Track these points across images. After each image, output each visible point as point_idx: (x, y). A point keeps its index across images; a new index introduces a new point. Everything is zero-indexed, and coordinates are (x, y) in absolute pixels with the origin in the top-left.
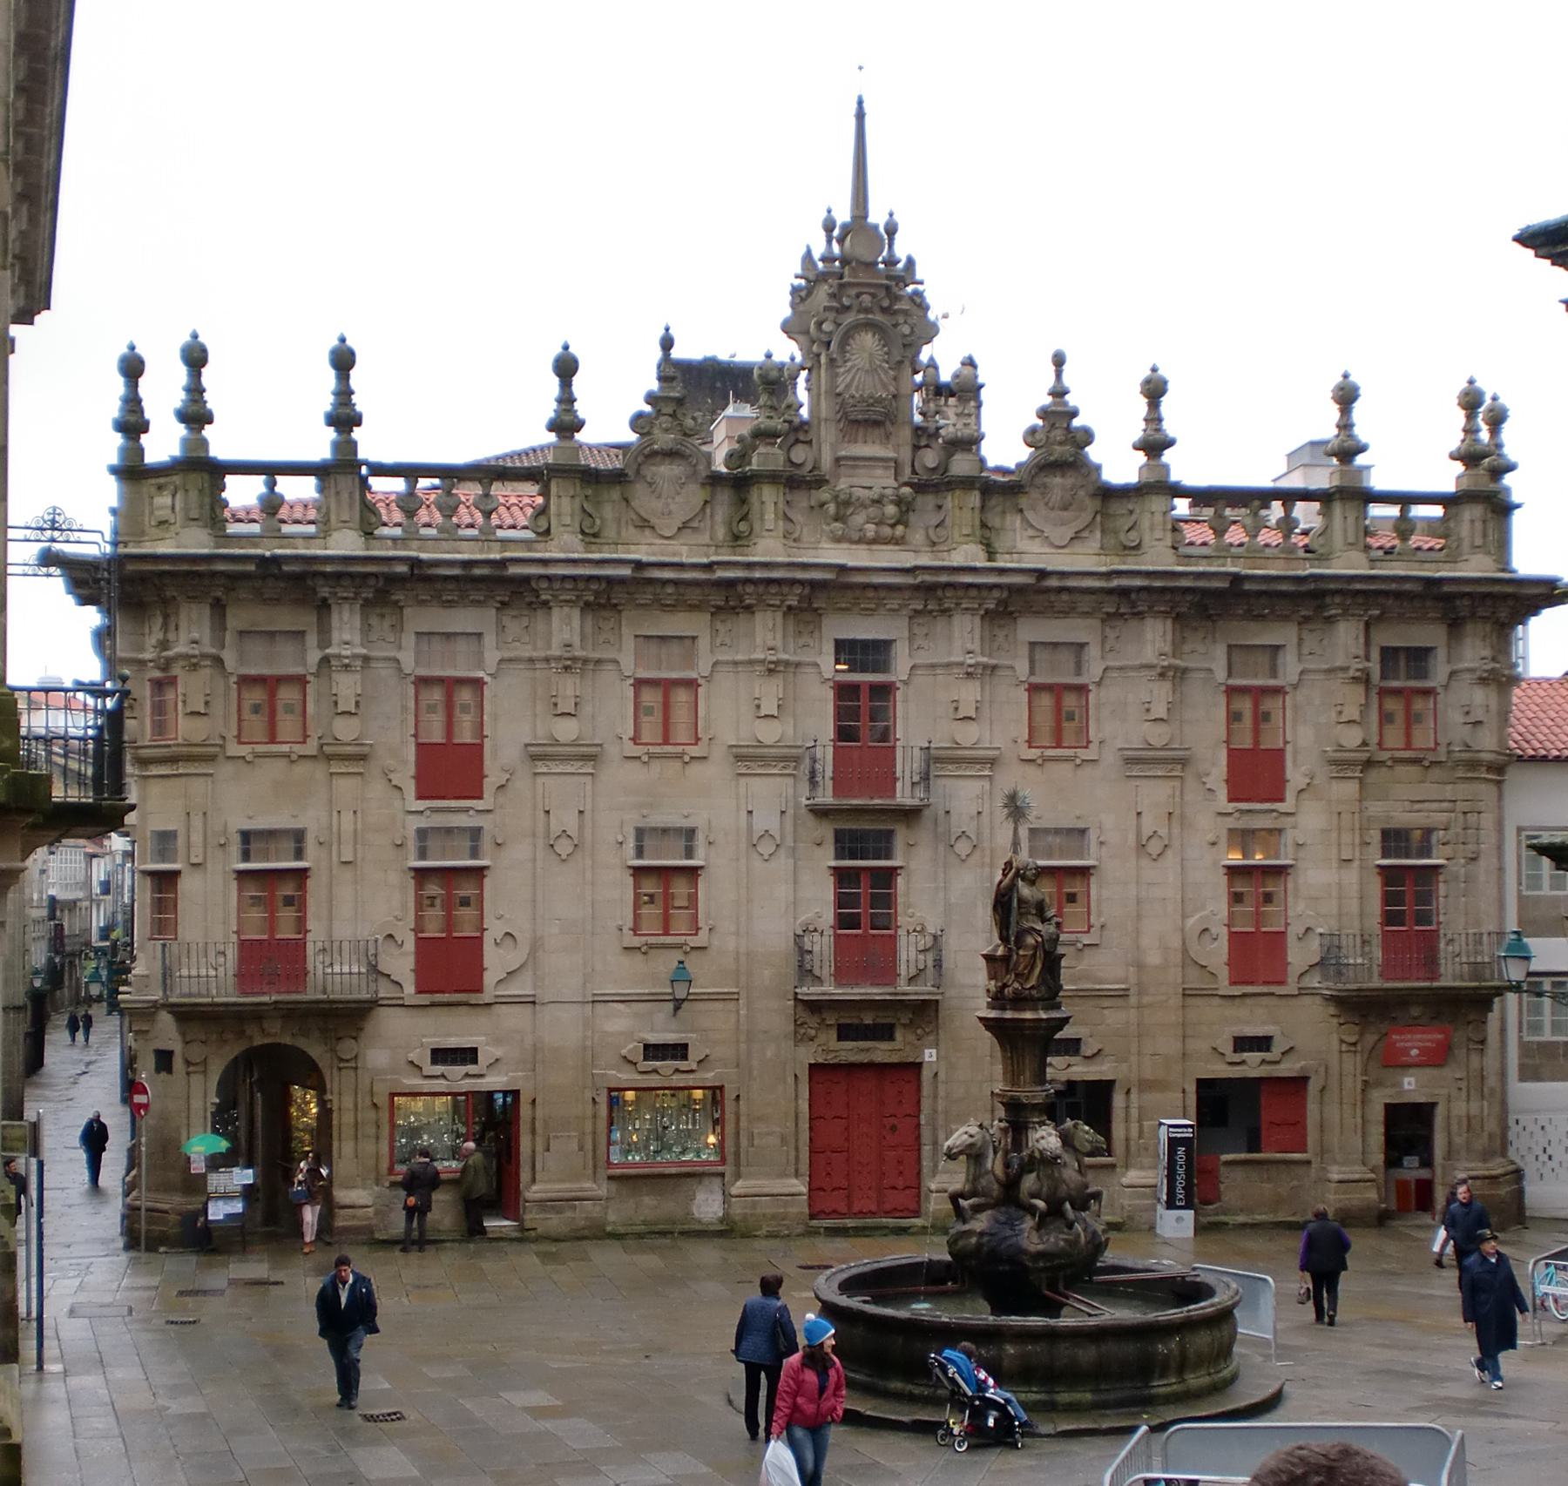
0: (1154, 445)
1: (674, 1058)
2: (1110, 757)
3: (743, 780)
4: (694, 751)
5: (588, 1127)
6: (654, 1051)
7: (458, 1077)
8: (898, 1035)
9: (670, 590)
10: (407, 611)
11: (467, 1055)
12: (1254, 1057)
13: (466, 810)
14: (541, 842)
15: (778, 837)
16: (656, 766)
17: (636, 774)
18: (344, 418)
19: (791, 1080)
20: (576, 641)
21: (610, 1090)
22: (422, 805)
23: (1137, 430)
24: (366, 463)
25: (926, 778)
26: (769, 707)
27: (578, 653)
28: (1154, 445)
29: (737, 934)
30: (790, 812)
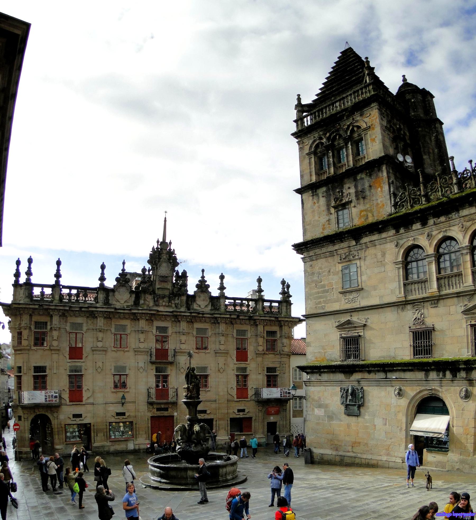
2: (212, 352)
4: (126, 349)
6: (118, 414)
7: (78, 421)
8: (169, 409)
9: (122, 315)
10: (68, 318)
11: (80, 416)
12: (241, 413)
13: (79, 362)
14: (94, 369)
16: (118, 353)
17: (114, 354)
21: (110, 423)
24: (61, 285)
25: (174, 356)
27: (103, 328)
29: (135, 389)
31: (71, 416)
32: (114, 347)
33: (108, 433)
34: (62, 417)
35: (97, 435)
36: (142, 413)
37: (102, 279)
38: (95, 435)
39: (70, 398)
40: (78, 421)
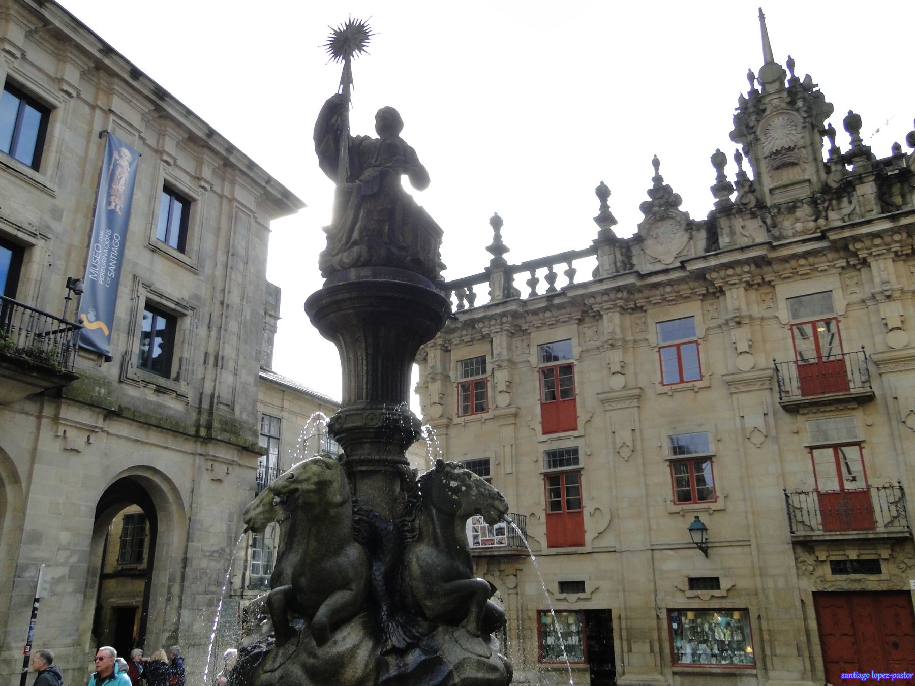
1: (712, 588)
3: (734, 396)
4: (699, 384)
5: (655, 635)
6: (696, 583)
7: (573, 601)
8: (884, 567)
10: (532, 335)
13: (568, 438)
15: (764, 430)
16: (678, 397)
18: (497, 248)
19: (798, 604)
20: (618, 330)
21: (670, 611)
26: (743, 346)
29: (744, 500)
30: (771, 414)
31: (555, 588)
32: (662, 383)
33: (667, 646)
35: (630, 650)
36: (781, 583)
37: (605, 219)
38: (625, 649)
39: (549, 535)
40: (573, 601)
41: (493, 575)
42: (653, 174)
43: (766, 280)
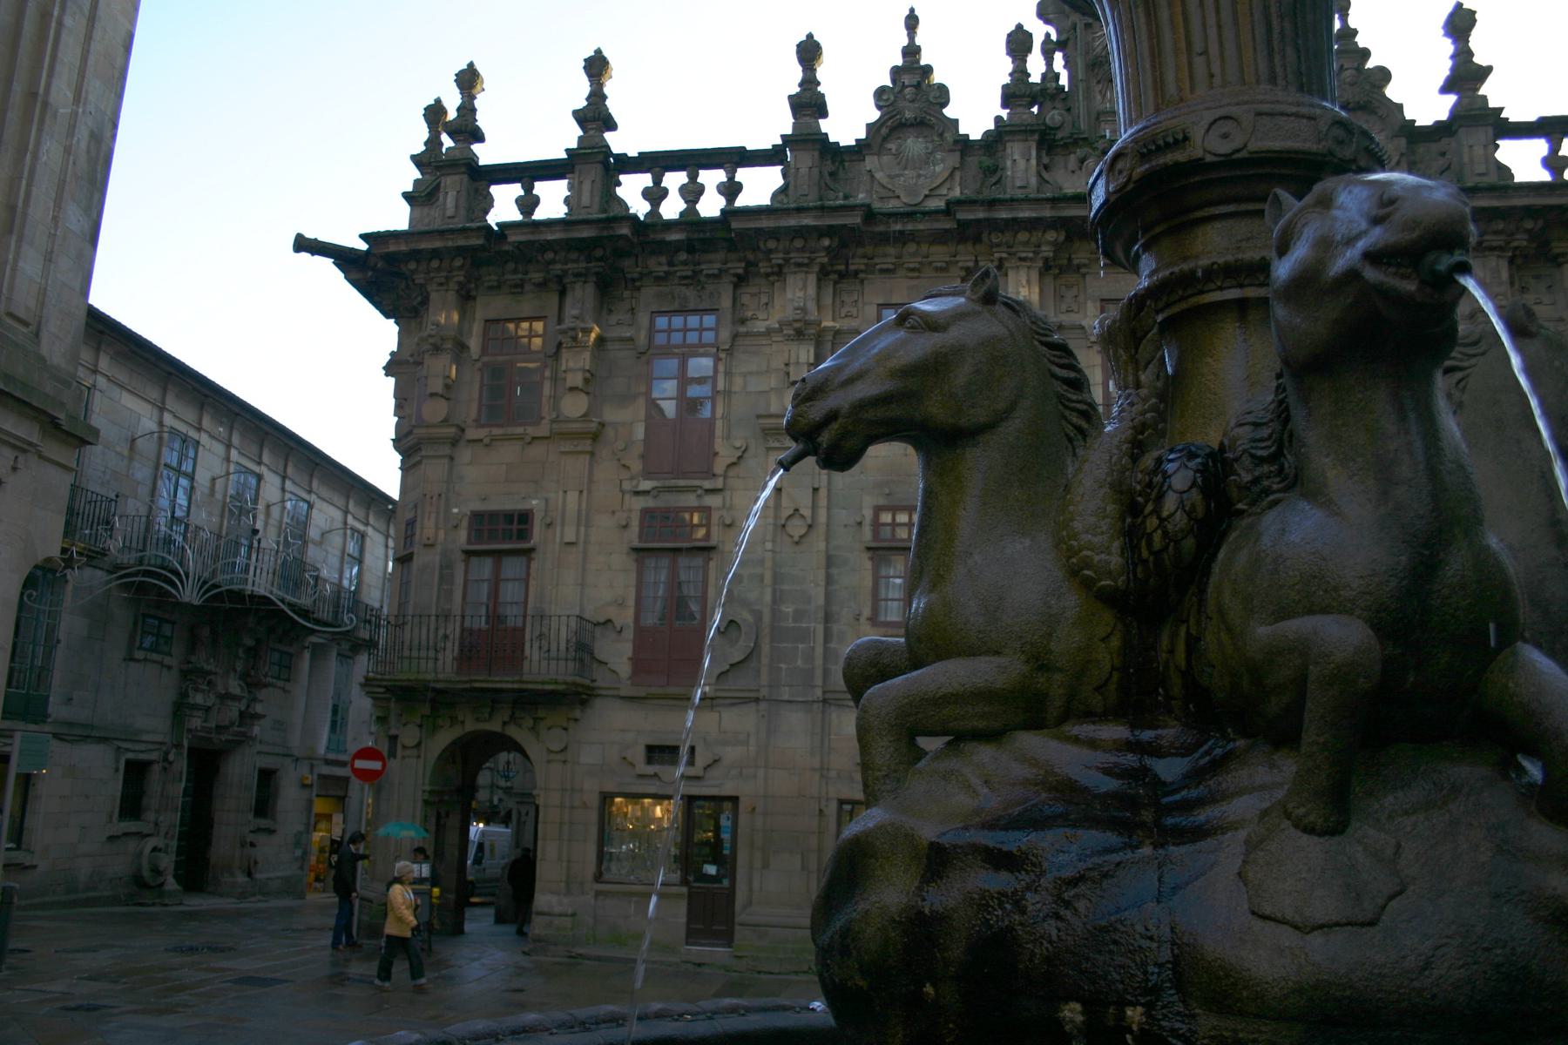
0: (1466, 76)
21: (841, 802)
22: (646, 485)
23: (1443, 68)
28: (1466, 76)
31: (639, 754)
34: (589, 756)
35: (766, 866)
37: (809, 104)
41: (520, 726)
42: (905, 42)
43: (1076, 262)
